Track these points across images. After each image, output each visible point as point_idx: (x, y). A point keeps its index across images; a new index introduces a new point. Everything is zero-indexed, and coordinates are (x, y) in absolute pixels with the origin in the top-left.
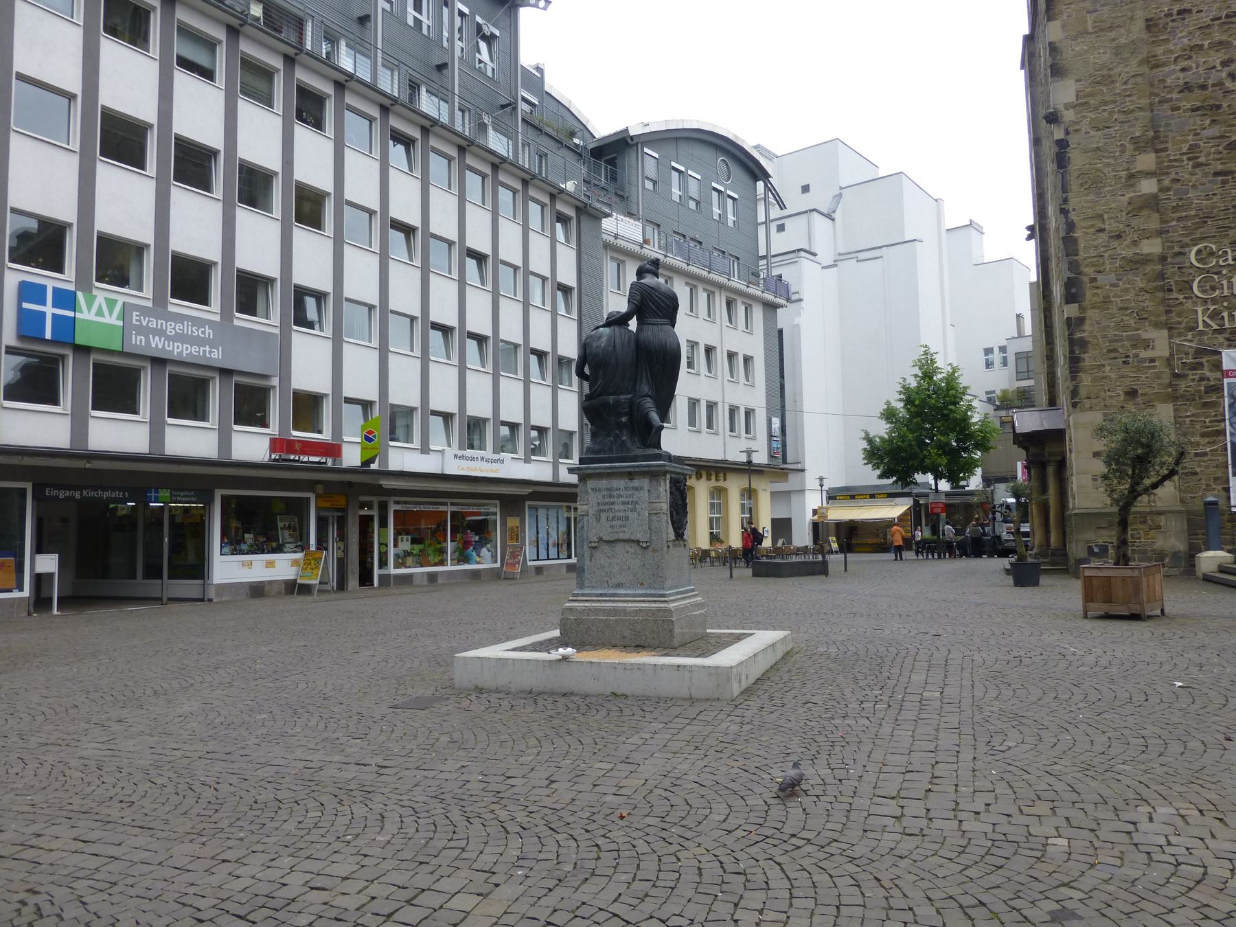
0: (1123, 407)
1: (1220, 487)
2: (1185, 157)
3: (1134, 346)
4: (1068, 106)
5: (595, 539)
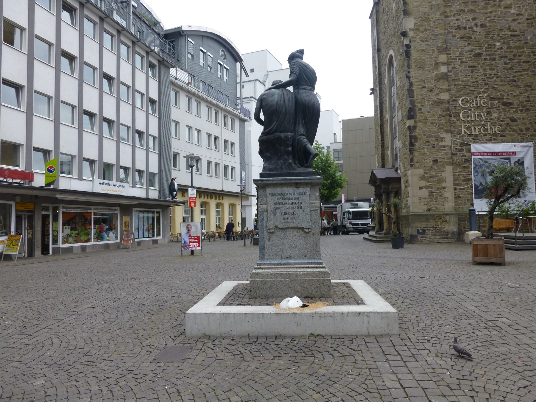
0: (432, 167)
1: (469, 203)
2: (457, 58)
3: (437, 140)
4: (411, 30)
5: (272, 227)
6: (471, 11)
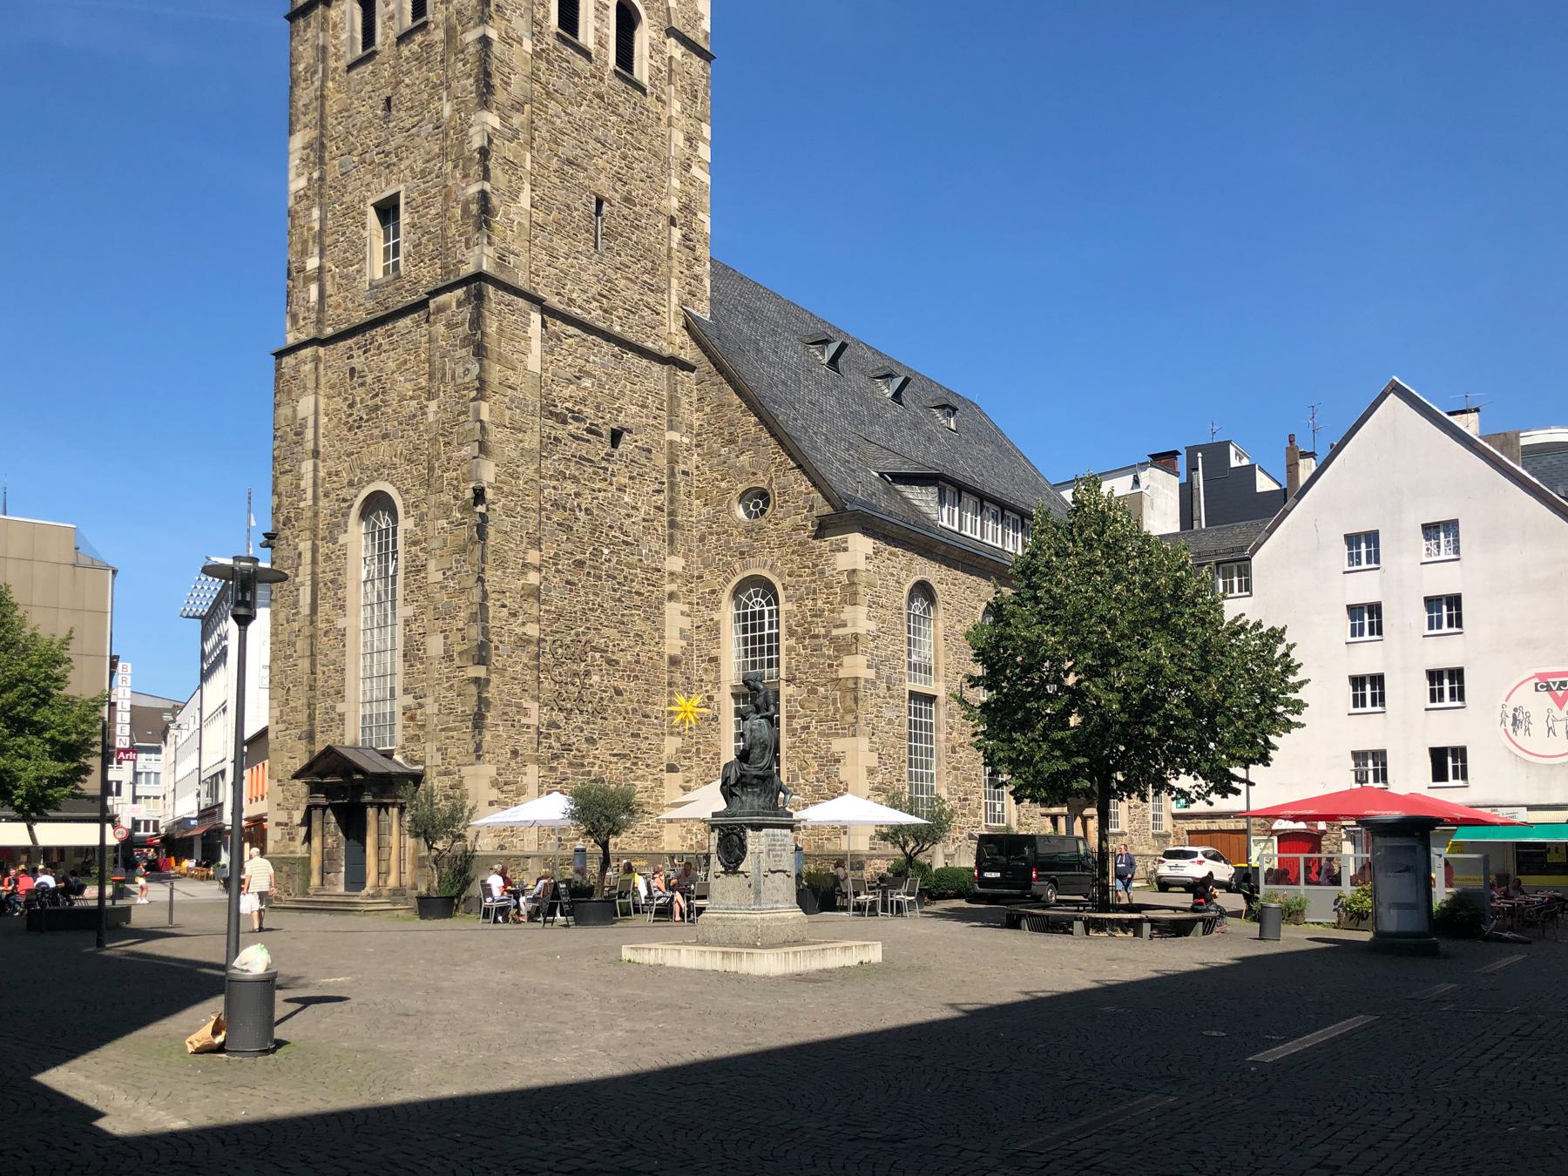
6: (575, 479)
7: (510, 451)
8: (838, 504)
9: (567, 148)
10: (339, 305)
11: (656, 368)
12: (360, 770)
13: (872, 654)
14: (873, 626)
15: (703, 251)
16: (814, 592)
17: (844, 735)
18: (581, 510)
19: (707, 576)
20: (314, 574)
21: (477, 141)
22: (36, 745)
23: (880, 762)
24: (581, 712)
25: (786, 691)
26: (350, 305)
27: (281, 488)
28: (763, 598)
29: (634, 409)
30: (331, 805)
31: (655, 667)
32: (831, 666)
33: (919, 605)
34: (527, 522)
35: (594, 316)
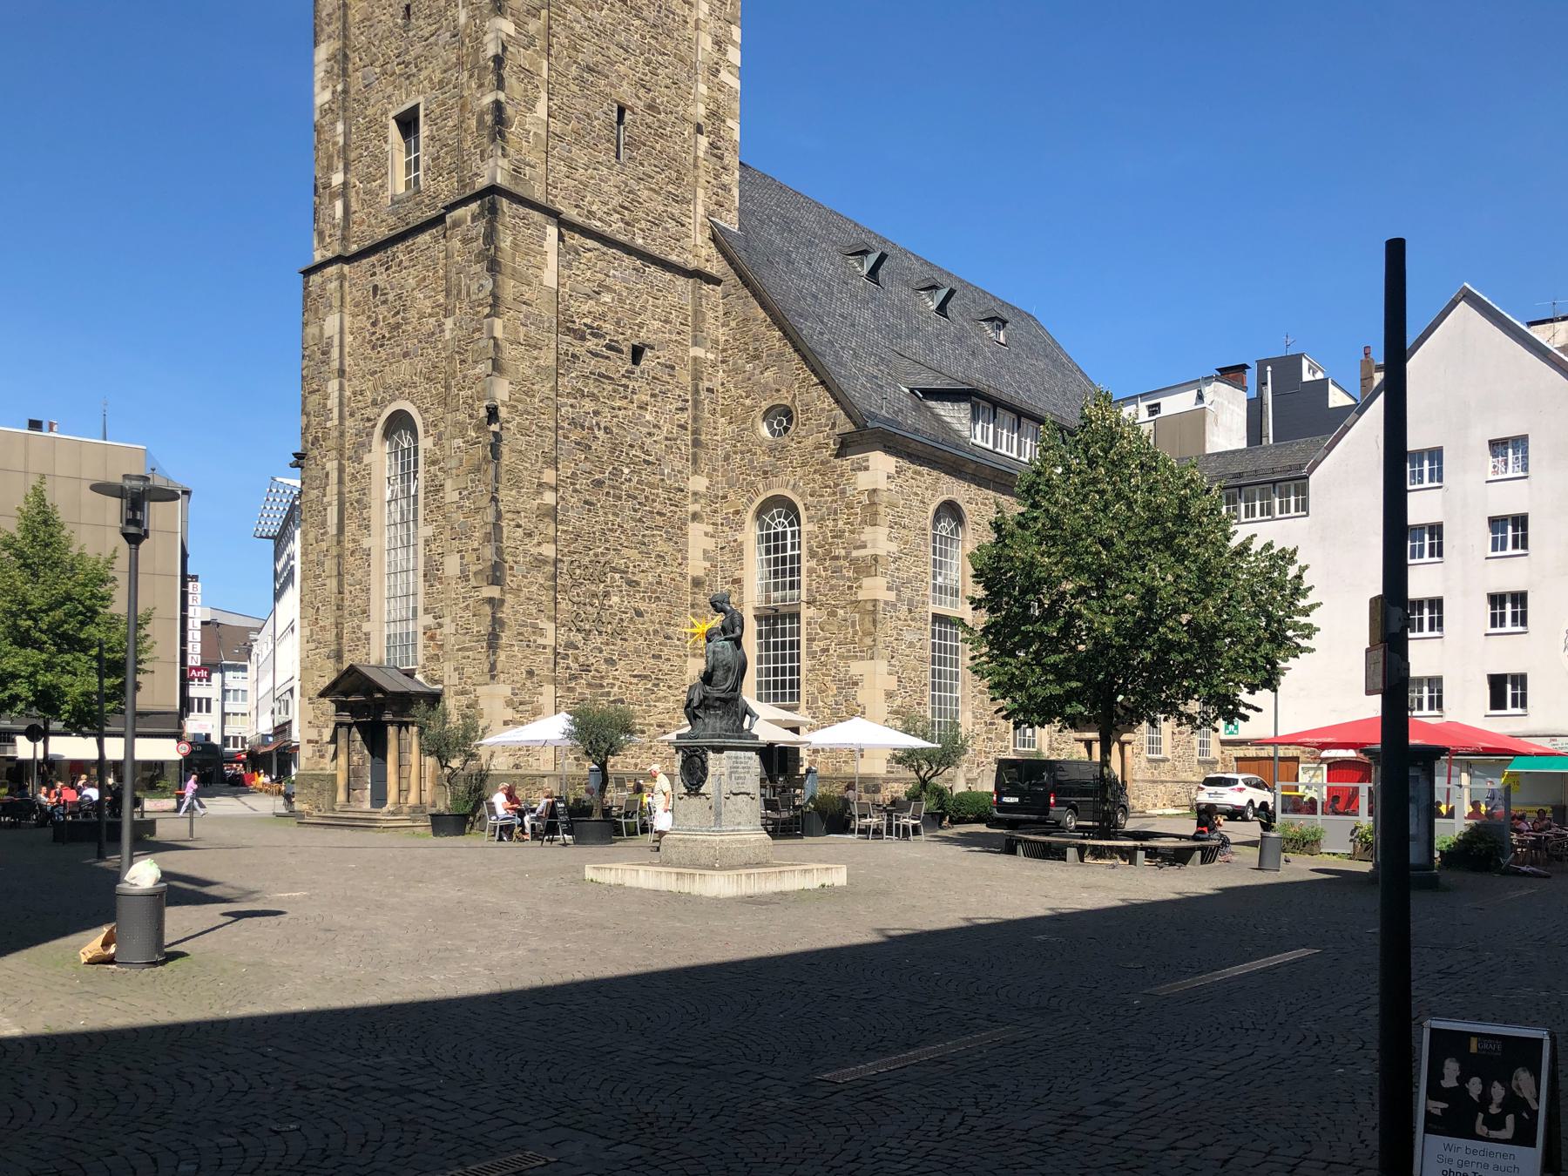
2: (569, 480)
7: (525, 369)
8: (860, 421)
9: (587, 55)
10: (363, 221)
11: (681, 281)
12: (381, 689)
13: (892, 576)
14: (893, 547)
15: (732, 160)
16: (836, 513)
17: (862, 658)
18: (599, 429)
19: (731, 496)
20: (340, 494)
21: (492, 49)
22: (83, 661)
23: (899, 686)
24: (600, 633)
25: (806, 613)
26: (373, 222)
27: (310, 408)
28: (786, 518)
29: (657, 324)
30: (357, 724)
31: (677, 588)
32: (850, 588)
33: (946, 525)
34: (543, 441)
35: (615, 229)
